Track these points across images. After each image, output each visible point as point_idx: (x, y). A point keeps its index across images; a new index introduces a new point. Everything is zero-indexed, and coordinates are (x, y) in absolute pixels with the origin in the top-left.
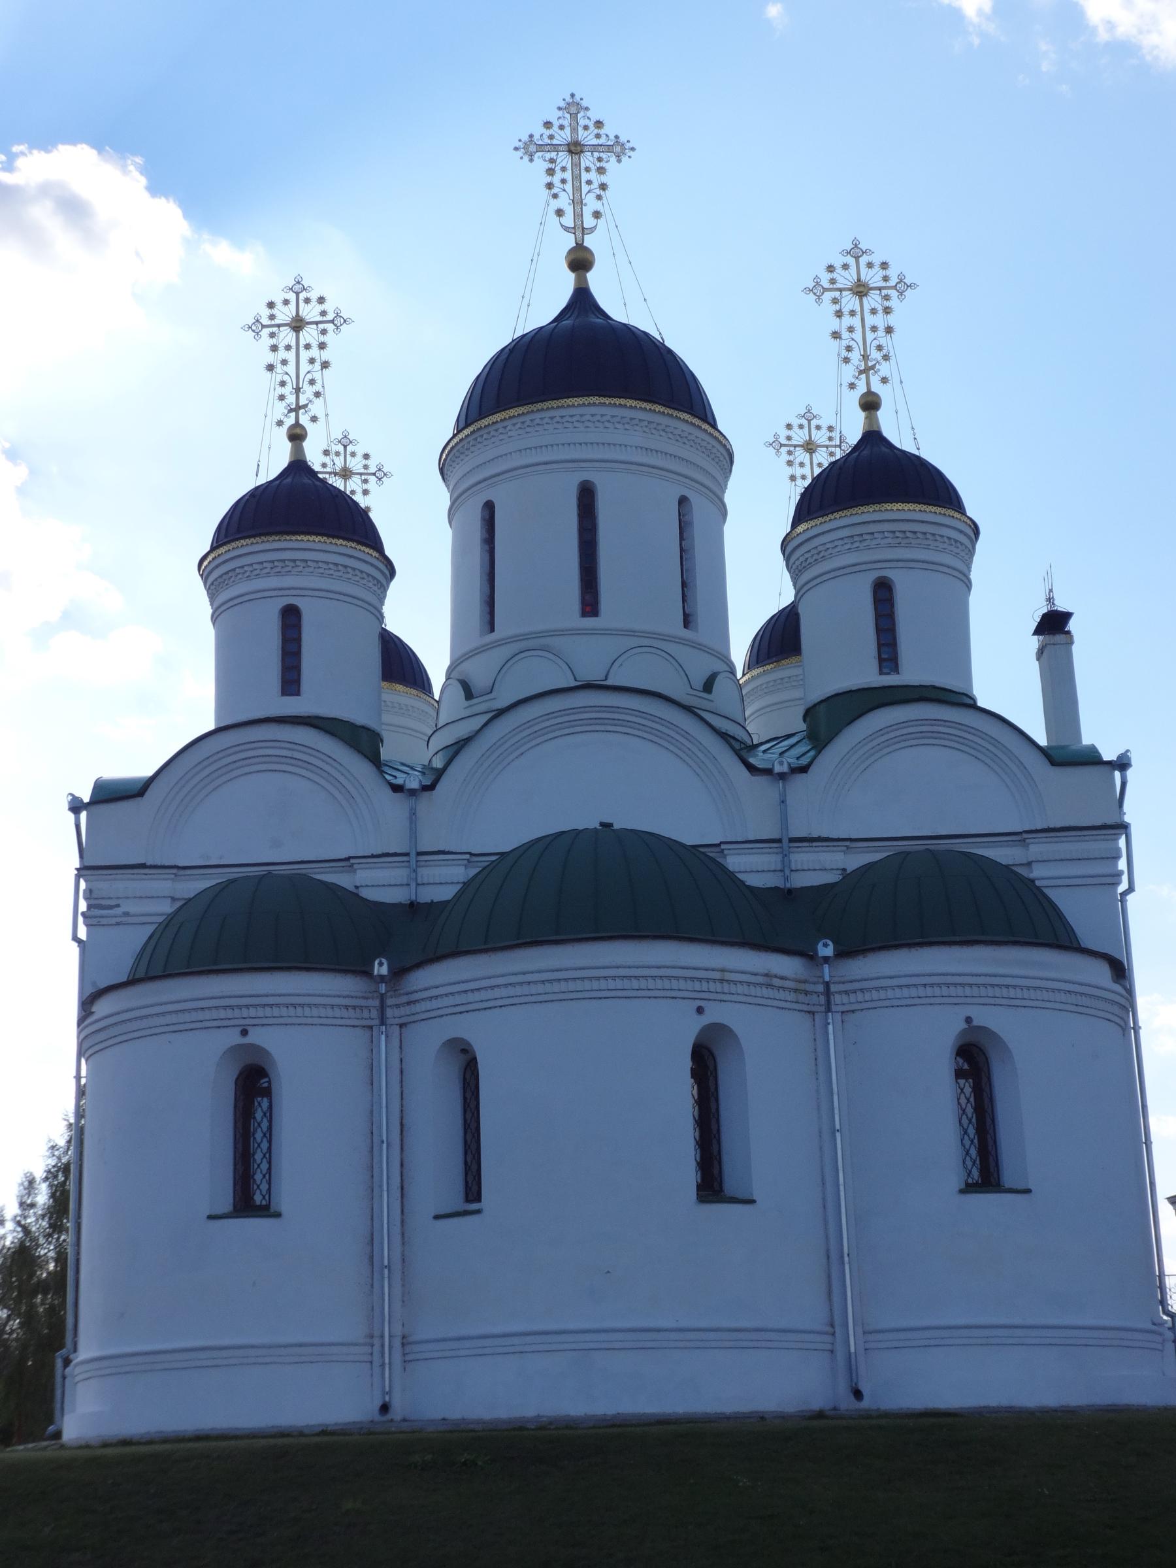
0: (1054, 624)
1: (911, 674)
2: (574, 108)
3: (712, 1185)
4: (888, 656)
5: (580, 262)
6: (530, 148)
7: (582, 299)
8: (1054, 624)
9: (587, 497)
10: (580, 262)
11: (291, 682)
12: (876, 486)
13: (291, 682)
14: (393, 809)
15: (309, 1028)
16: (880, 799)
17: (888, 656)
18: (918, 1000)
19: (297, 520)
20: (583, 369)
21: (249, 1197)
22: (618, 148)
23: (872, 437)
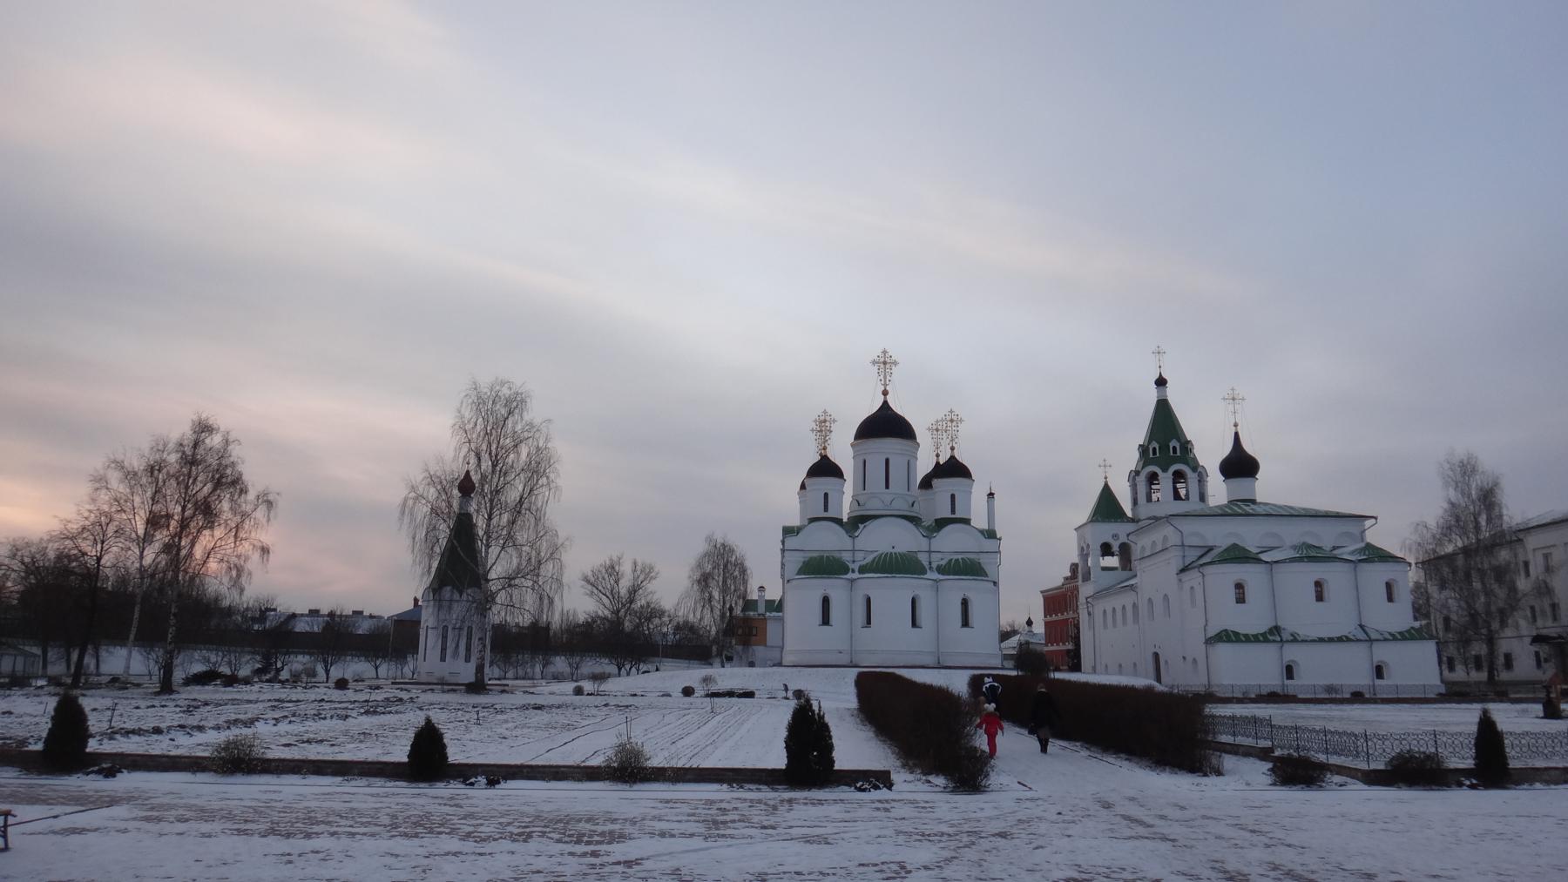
0: (991, 495)
1: (958, 515)
2: (885, 352)
3: (914, 624)
4: (953, 511)
5: (885, 393)
6: (874, 362)
7: (885, 402)
8: (991, 495)
9: (887, 461)
10: (885, 393)
11: (826, 509)
12: (953, 469)
13: (826, 509)
14: (848, 541)
15: (835, 588)
16: (951, 542)
17: (953, 511)
18: (956, 588)
19: (825, 468)
20: (885, 425)
21: (826, 620)
22: (895, 363)
23: (952, 457)
